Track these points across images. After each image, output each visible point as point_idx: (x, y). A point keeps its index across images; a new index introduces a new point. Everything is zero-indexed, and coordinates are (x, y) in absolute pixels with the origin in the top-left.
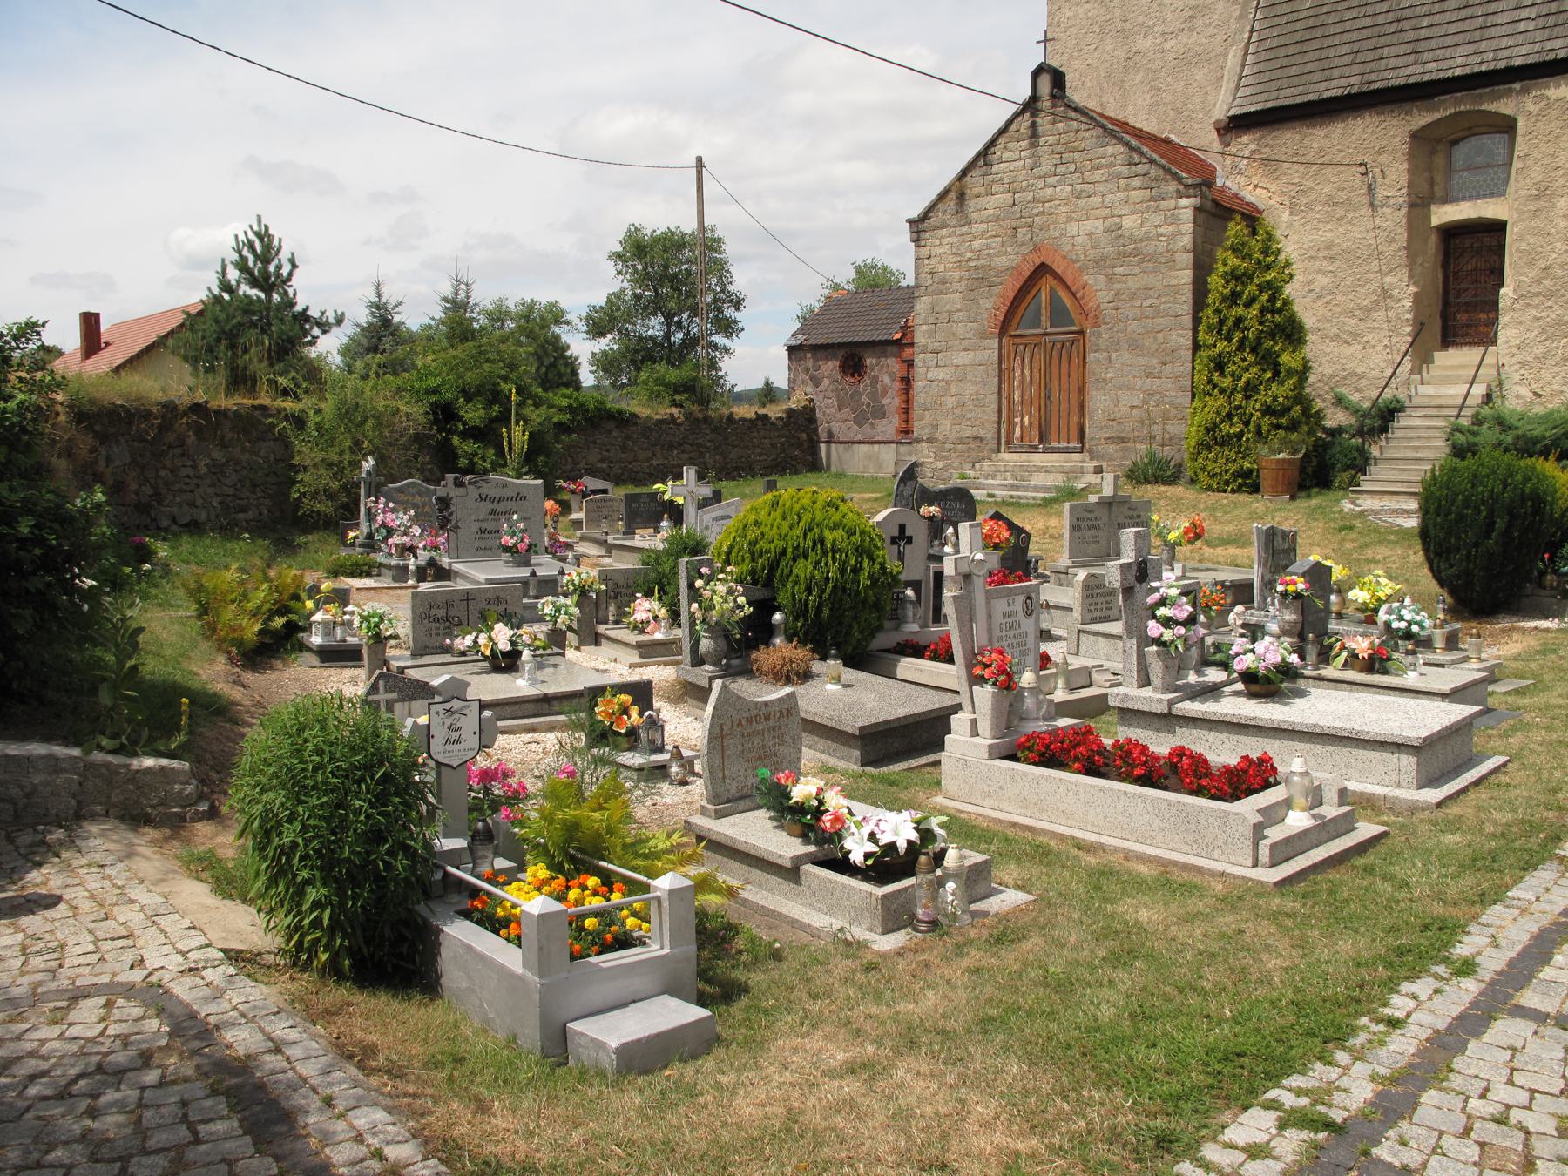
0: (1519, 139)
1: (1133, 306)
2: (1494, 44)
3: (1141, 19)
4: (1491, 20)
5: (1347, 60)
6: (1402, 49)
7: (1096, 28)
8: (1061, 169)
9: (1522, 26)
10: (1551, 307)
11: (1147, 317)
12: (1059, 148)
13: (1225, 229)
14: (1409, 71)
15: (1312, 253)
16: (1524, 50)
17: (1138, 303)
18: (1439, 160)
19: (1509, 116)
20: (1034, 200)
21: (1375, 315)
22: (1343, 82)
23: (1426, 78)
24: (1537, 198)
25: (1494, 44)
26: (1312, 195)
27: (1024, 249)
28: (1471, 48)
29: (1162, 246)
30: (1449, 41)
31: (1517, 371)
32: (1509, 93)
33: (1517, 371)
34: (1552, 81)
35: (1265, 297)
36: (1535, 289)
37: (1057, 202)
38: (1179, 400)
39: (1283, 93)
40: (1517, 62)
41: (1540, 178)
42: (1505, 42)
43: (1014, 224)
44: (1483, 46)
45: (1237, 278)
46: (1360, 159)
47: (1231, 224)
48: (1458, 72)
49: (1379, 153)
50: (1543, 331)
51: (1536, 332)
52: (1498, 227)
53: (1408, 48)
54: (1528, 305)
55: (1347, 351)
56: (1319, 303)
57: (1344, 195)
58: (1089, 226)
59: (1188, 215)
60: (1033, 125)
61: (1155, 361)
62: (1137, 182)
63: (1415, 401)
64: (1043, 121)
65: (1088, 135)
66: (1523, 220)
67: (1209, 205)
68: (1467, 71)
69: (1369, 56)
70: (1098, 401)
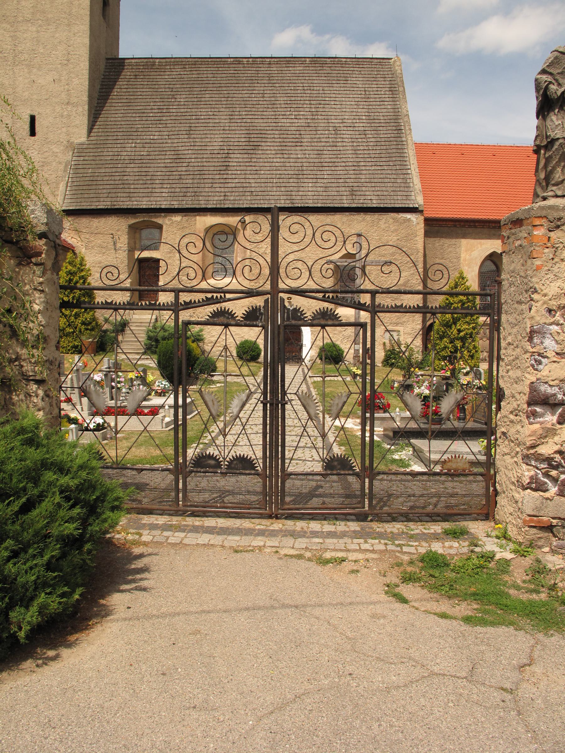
0: (164, 232)
2: (155, 199)
4: (154, 190)
5: (105, 195)
6: (125, 195)
9: (164, 194)
13: (66, 255)
14: (128, 203)
16: (165, 203)
18: (137, 235)
22: (104, 203)
23: (134, 207)
25: (155, 199)
26: (93, 244)
28: (148, 199)
30: (141, 195)
32: (160, 216)
35: (82, 281)
39: (82, 204)
40: (163, 207)
42: (159, 199)
44: (152, 199)
45: (71, 274)
46: (111, 232)
47: (69, 254)
48: (144, 207)
49: (118, 231)
52: (158, 261)
53: (127, 195)
63: (133, 321)
68: (147, 207)
69: (113, 195)
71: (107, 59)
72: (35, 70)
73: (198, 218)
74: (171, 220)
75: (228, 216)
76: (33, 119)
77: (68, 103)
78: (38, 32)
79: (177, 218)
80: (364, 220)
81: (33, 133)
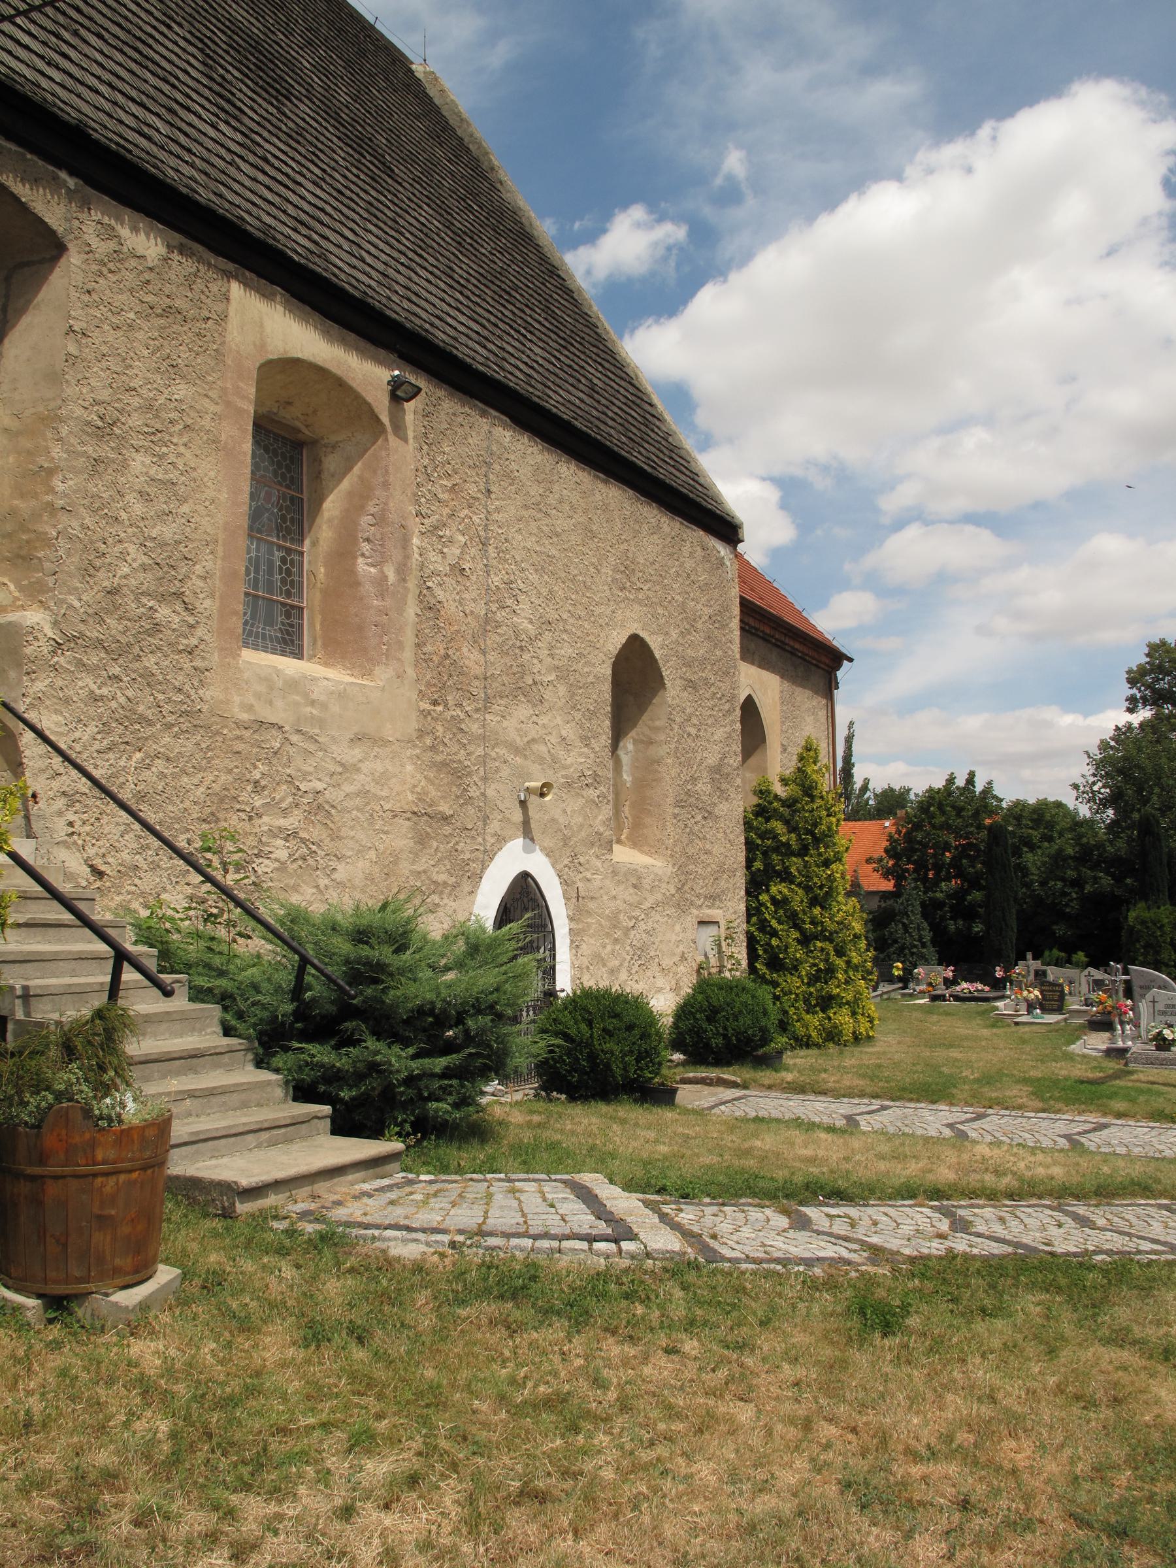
10: (118, 678)
19: (53, 233)
31: (60, 814)
32: (55, 184)
33: (60, 814)
34: (127, 214)
36: (93, 633)
41: (105, 395)
50: (105, 729)
51: (92, 729)
54: (81, 664)
66: (76, 472)
73: (236, 288)
74: (113, 236)
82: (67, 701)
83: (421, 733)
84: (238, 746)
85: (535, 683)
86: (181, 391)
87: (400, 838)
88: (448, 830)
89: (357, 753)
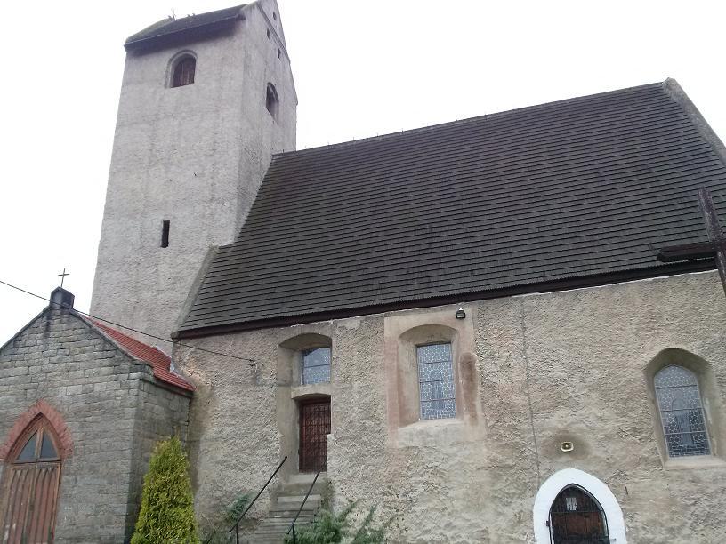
0: (334, 349)
1: (95, 443)
3: (146, 282)
7: (121, 285)
8: (60, 352)
11: (103, 451)
12: (61, 339)
15: (222, 413)
17: (98, 441)
20: (42, 371)
21: (258, 452)
24: (344, 382)
27: (30, 404)
29: (118, 402)
37: (55, 373)
38: (118, 510)
43: (26, 386)
49: (261, 355)
50: (351, 460)
52: (326, 400)
55: (241, 476)
56: (226, 444)
57: (242, 379)
58: (72, 389)
59: (134, 383)
60: (48, 325)
61: (105, 482)
62: (106, 362)
64: (55, 323)
65: (77, 331)
67: (151, 378)
70: (65, 511)
71: (273, 155)
72: (173, 168)
75: (435, 311)
76: (166, 225)
77: (212, 200)
78: (180, 125)
79: (353, 323)
80: (685, 285)
81: (165, 243)
82: (339, 455)
83: (489, 436)
84: (401, 457)
85: (570, 397)
86: (369, 358)
87: (484, 477)
88: (513, 471)
89: (455, 449)
